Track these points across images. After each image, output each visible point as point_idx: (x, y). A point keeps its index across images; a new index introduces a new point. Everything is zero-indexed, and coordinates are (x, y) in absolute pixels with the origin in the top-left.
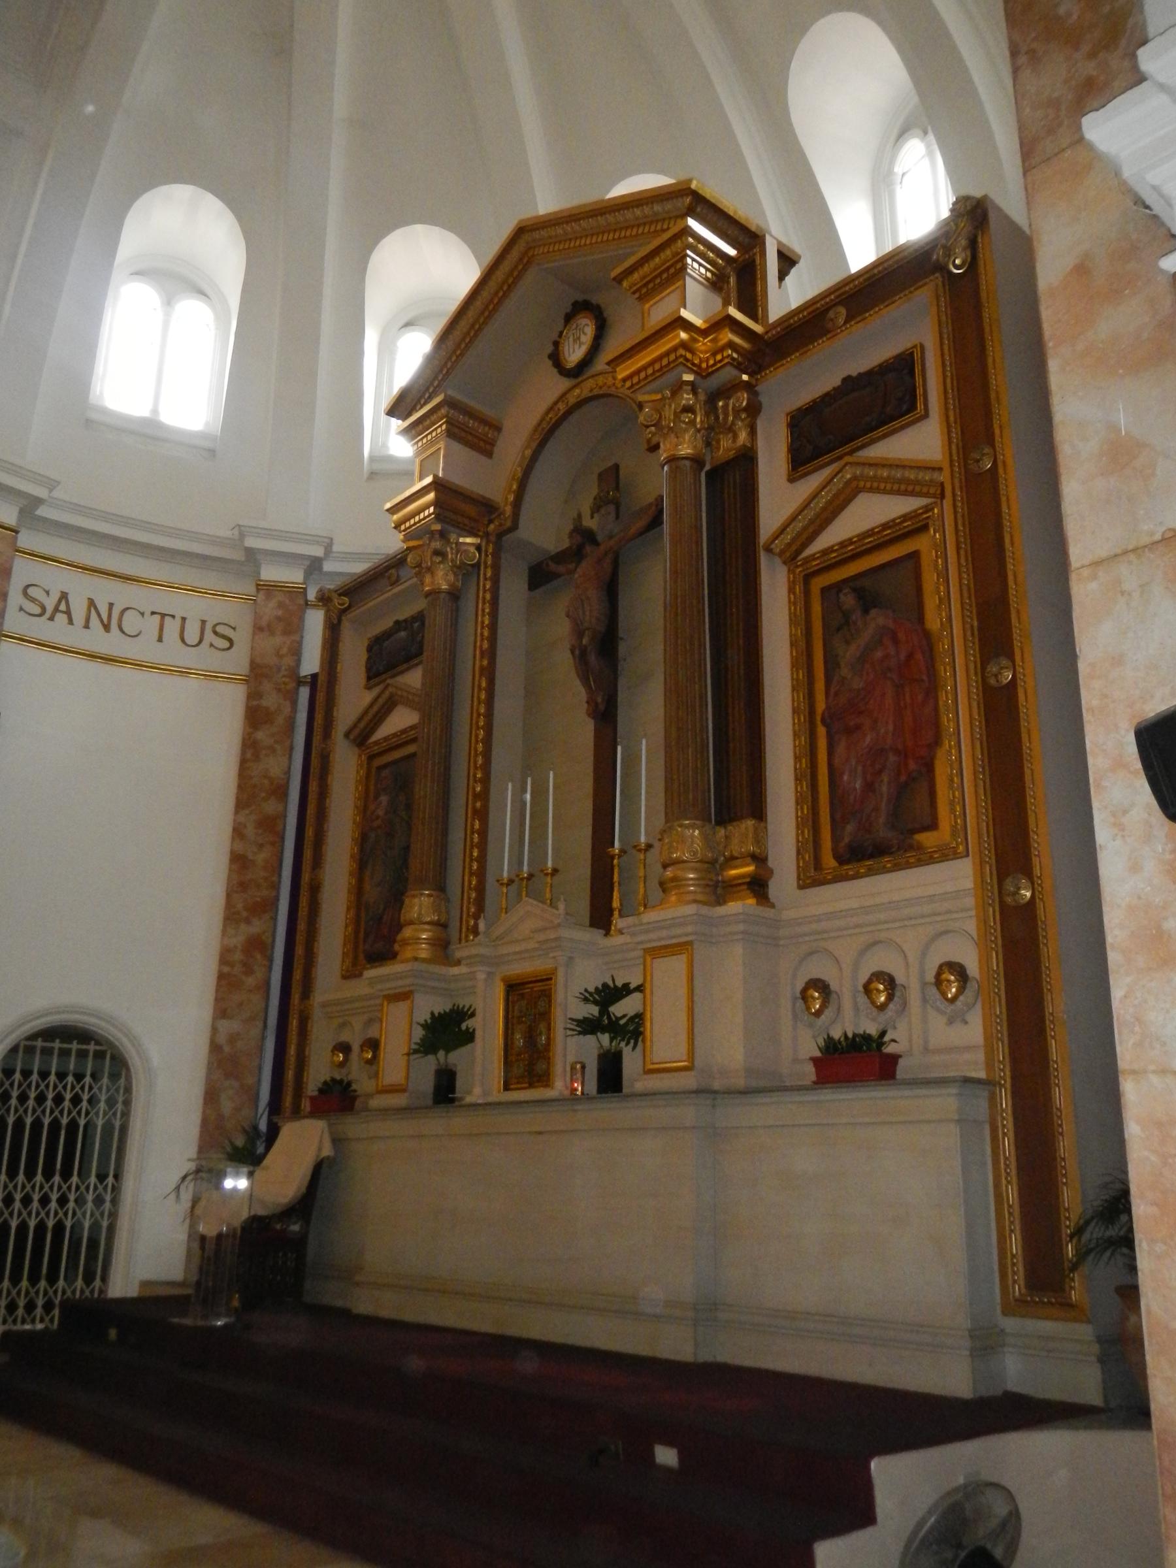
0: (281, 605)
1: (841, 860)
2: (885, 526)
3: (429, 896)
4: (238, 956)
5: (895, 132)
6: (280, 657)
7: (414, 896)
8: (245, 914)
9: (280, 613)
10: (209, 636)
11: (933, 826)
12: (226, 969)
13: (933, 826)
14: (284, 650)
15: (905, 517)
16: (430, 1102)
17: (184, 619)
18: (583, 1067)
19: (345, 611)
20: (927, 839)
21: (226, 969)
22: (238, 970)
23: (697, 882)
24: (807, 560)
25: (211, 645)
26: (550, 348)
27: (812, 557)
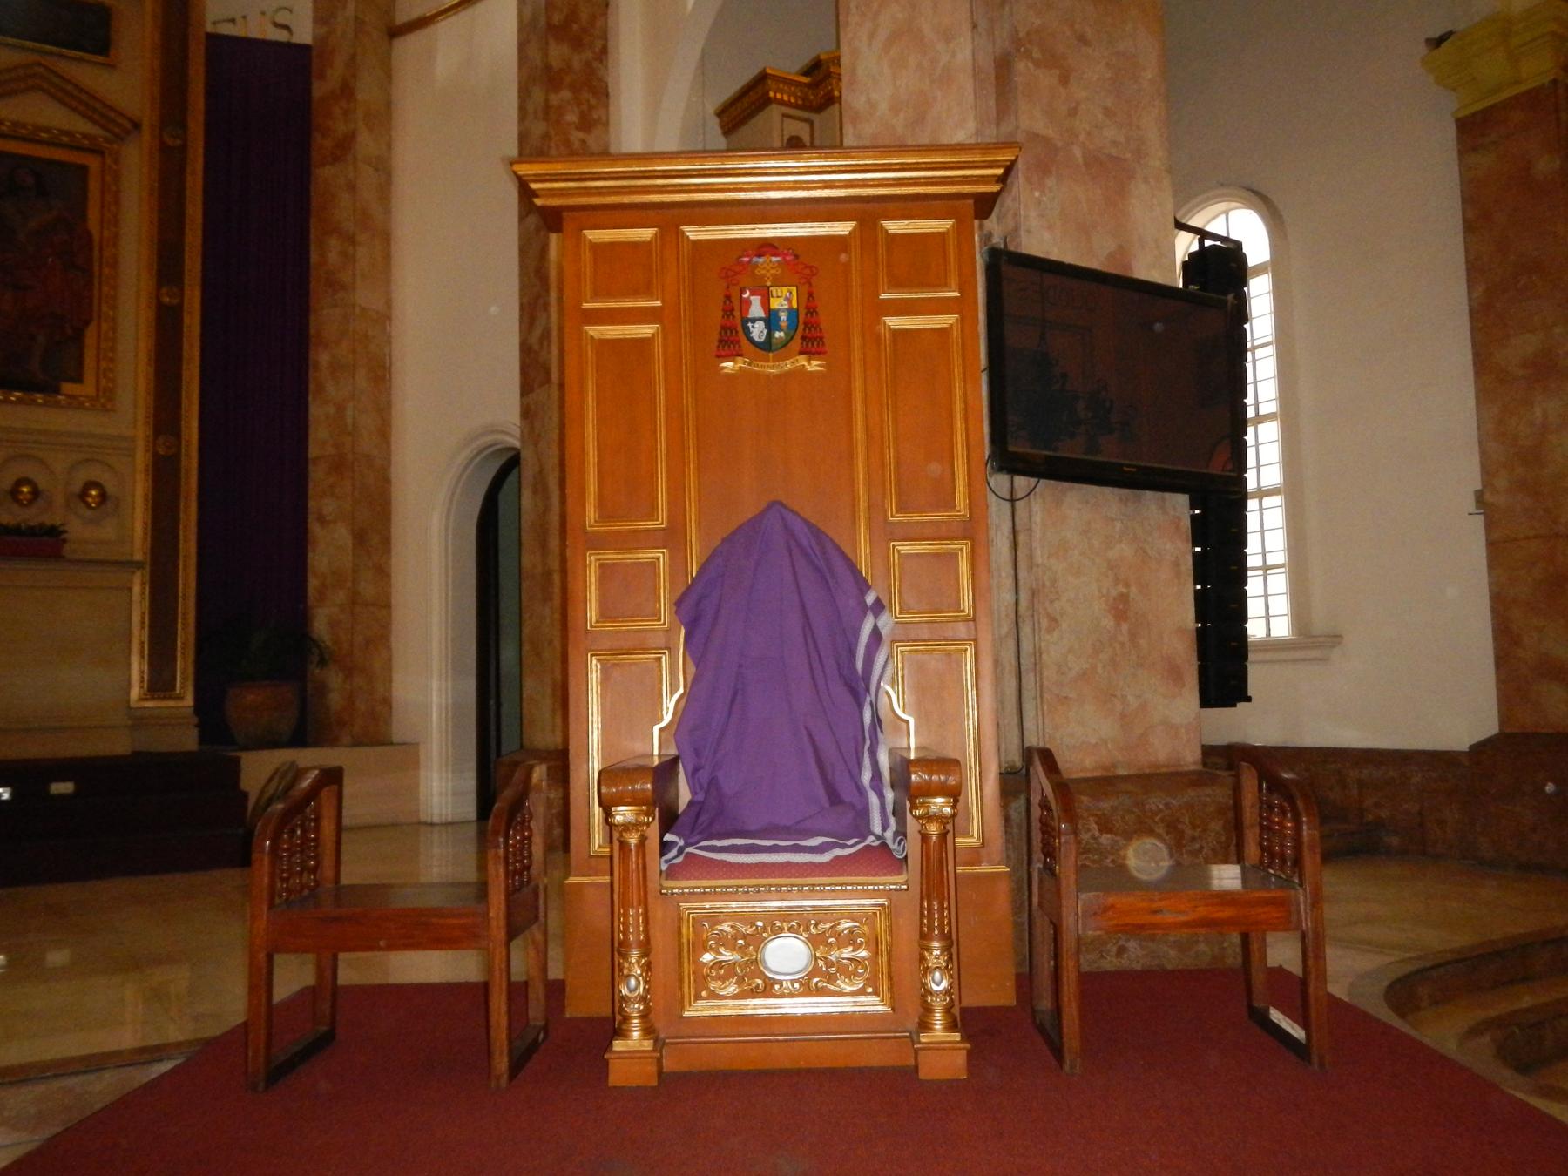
11: (78, 378)
15: (85, 136)
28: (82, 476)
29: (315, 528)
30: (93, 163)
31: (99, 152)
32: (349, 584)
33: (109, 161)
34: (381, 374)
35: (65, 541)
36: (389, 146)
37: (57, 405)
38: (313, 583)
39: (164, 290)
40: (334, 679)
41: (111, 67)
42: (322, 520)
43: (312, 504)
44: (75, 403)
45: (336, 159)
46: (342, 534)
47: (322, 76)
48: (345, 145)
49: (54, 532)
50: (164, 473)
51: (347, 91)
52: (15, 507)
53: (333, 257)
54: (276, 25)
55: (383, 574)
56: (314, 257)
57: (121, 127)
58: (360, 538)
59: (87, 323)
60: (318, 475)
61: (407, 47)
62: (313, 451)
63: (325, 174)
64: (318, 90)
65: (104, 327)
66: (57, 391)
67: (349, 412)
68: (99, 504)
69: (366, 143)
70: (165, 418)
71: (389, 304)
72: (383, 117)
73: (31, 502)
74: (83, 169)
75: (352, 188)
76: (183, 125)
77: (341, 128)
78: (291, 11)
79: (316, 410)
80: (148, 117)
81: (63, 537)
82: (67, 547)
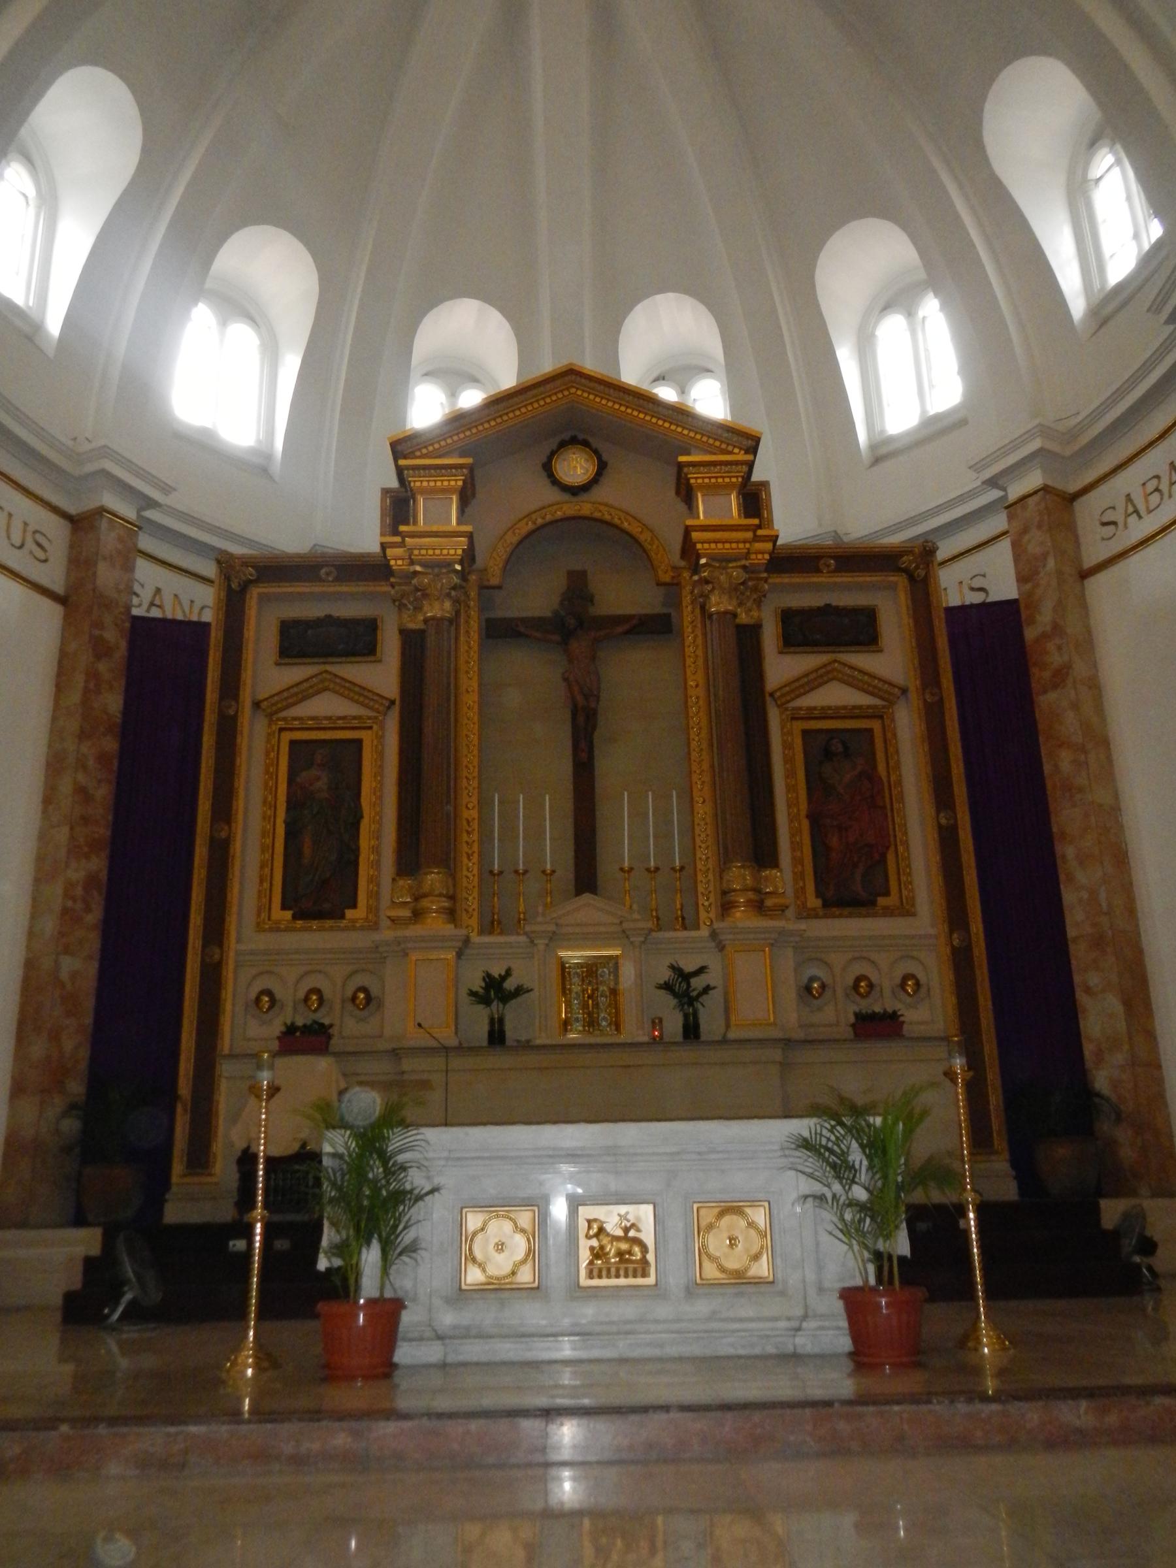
0: (120, 539)
1: (826, 904)
2: (854, 707)
3: (438, 873)
4: (79, 891)
5: (655, 375)
6: (119, 592)
7: (426, 874)
8: (86, 849)
9: (120, 546)
10: (30, 545)
11: (887, 893)
12: (70, 904)
13: (887, 893)
14: (122, 587)
15: (869, 707)
16: (485, 1043)
17: (10, 515)
18: (661, 1020)
19: (251, 581)
20: (882, 901)
21: (70, 904)
22: (79, 906)
23: (736, 904)
24: (794, 709)
25: (31, 552)
26: (544, 459)
27: (800, 709)
28: (859, 969)
29: (1081, 997)
30: (876, 725)
31: (881, 717)
32: (1126, 1047)
33: (887, 722)
34: (1121, 858)
35: (903, 1022)
36: (1095, 665)
37: (875, 915)
38: (1088, 1049)
39: (942, 815)
40: (1123, 1135)
41: (881, 651)
42: (1088, 990)
43: (1077, 979)
44: (888, 912)
45: (1055, 686)
46: (1113, 1003)
47: (1032, 621)
48: (1061, 676)
49: (894, 1016)
50: (961, 960)
51: (1057, 629)
52: (857, 998)
53: (1066, 765)
54: (972, 589)
55: (1150, 1035)
56: (1047, 768)
57: (889, 693)
58: (1127, 1004)
59: (888, 848)
60: (1079, 953)
61: (1098, 585)
62: (1071, 933)
63: (1046, 701)
64: (1030, 634)
65: (901, 849)
66: (873, 903)
67: (1103, 895)
68: (916, 991)
69: (1080, 668)
70: (956, 916)
71: (1116, 796)
72: (1087, 644)
73: (820, 995)
74: (870, 731)
75: (1075, 706)
76: (938, 684)
77: (1056, 659)
78: (984, 576)
79: (1069, 897)
80: (913, 684)
81: (902, 1019)
82: (905, 1027)
